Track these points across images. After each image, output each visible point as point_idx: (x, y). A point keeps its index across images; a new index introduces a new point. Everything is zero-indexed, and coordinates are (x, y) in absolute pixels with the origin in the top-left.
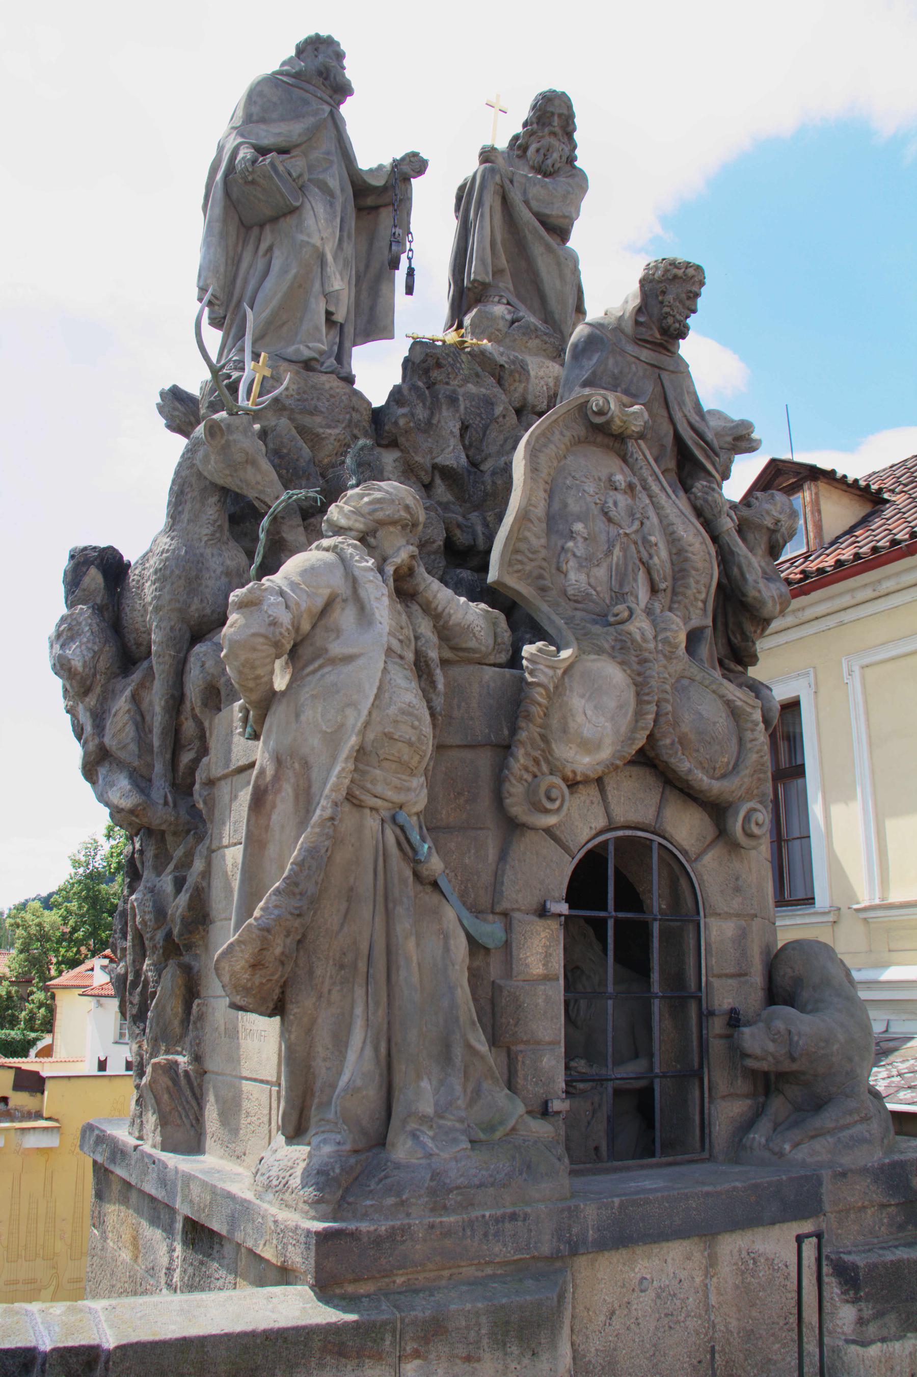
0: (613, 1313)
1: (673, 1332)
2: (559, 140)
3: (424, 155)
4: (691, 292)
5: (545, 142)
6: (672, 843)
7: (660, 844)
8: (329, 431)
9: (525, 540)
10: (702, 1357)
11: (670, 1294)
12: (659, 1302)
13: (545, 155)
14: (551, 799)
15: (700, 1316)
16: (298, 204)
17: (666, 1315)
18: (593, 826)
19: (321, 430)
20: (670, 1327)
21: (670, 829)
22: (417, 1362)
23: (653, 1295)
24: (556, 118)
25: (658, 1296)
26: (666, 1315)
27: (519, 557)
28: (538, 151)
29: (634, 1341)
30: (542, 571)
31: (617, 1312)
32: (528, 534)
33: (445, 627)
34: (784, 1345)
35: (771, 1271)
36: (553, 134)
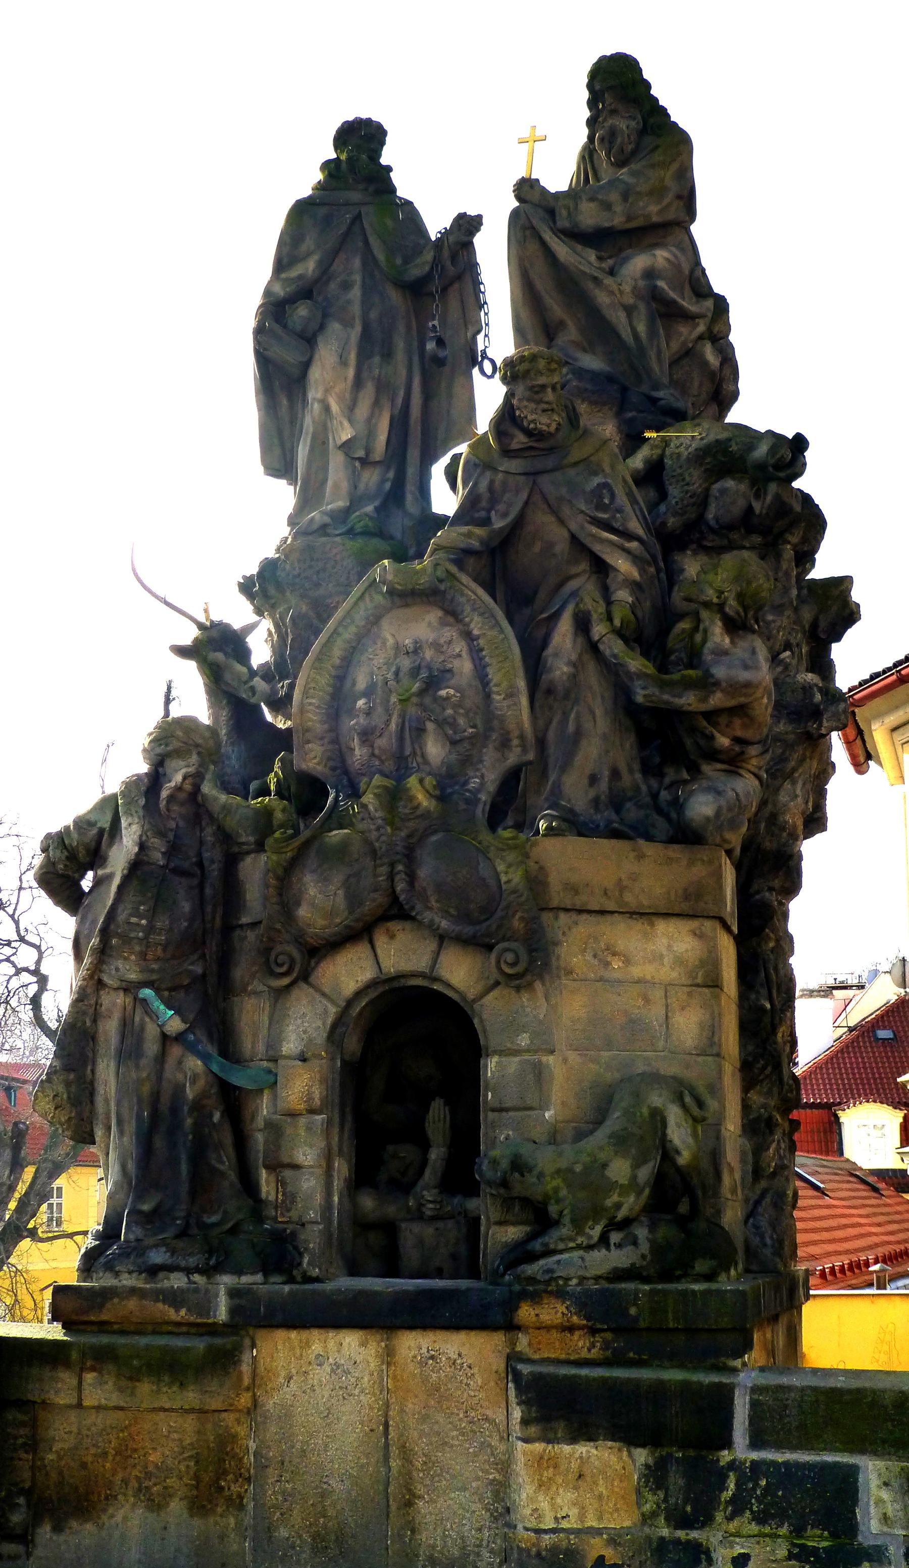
0: (291, 1378)
1: (345, 1402)
3: (472, 212)
4: (533, 387)
10: (374, 1427)
11: (344, 1371)
12: (333, 1376)
15: (374, 1394)
17: (341, 1388)
18: (359, 979)
20: (344, 1398)
22: (95, 1374)
23: (328, 1370)
25: (333, 1371)
26: (341, 1388)
29: (309, 1403)
35: (452, 1369)
36: (614, 112)
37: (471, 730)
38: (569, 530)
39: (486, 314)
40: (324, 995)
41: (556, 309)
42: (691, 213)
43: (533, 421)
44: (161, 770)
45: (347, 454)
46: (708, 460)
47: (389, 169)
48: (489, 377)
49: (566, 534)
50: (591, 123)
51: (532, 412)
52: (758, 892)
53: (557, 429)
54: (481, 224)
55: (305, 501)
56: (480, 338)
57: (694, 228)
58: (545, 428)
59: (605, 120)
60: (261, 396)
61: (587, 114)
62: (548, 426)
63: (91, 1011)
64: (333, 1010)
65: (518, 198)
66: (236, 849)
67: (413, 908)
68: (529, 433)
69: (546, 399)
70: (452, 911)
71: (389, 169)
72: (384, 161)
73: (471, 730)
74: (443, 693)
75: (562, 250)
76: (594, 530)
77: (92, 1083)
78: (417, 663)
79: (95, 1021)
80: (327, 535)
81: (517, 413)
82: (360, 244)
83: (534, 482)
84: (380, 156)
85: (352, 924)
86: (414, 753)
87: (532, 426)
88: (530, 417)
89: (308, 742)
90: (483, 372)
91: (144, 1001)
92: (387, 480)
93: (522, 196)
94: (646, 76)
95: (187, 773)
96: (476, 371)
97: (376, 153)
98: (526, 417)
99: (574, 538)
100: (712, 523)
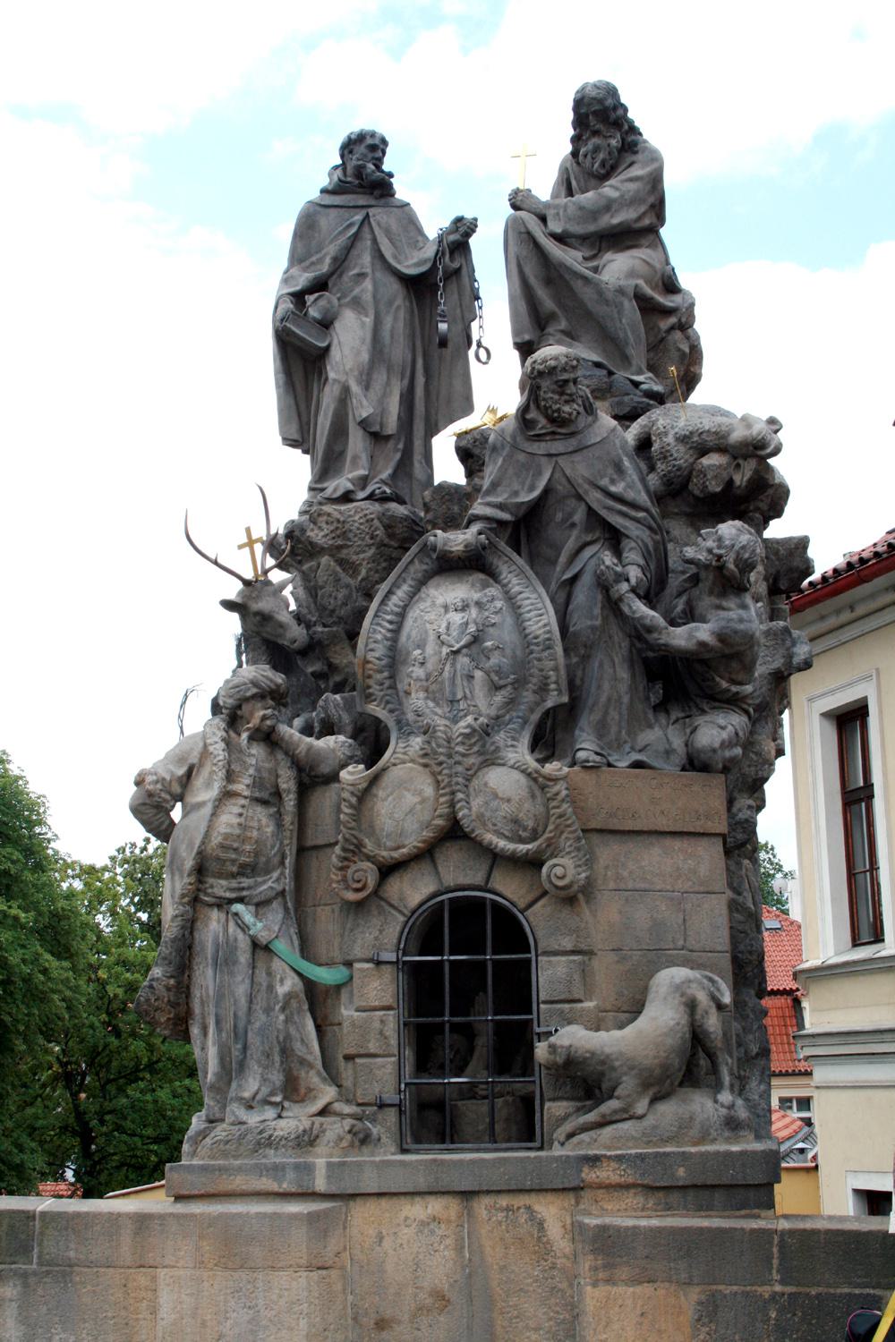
2: (605, 137)
3: (469, 215)
5: (590, 146)
6: (504, 898)
7: (491, 900)
8: (362, 556)
9: (370, 677)
13: (593, 158)
14: (359, 881)
16: (324, 345)
19: (355, 557)
21: (499, 887)
24: (591, 117)
27: (371, 691)
28: (585, 156)
30: (388, 698)
31: (386, 1238)
32: (371, 672)
33: (298, 761)
34: (536, 1281)
37: (512, 677)
38: (587, 503)
39: (480, 308)
40: (392, 906)
41: (548, 303)
42: (661, 218)
43: (558, 410)
44: (239, 712)
45: (364, 429)
46: (695, 439)
47: (391, 175)
48: (485, 363)
49: (583, 507)
50: (576, 140)
51: (556, 403)
52: (740, 810)
53: (576, 417)
54: (476, 226)
55: (324, 471)
56: (475, 325)
57: (663, 232)
58: (567, 416)
59: (588, 139)
60: (281, 376)
61: (571, 132)
62: (570, 414)
63: (189, 925)
64: (402, 919)
65: (515, 207)
66: (306, 780)
67: (473, 831)
68: (552, 420)
69: (569, 392)
70: (507, 833)
71: (391, 175)
72: (386, 167)
73: (512, 677)
74: (489, 644)
75: (555, 250)
76: (611, 503)
77: (188, 987)
78: (465, 620)
79: (191, 933)
80: (352, 501)
81: (543, 403)
82: (369, 243)
83: (557, 462)
84: (382, 163)
85: (420, 845)
86: (465, 697)
87: (556, 415)
88: (555, 407)
89: (369, 687)
90: (478, 359)
91: (236, 914)
92: (398, 450)
93: (518, 203)
94: (623, 100)
95: (264, 715)
96: (471, 353)
97: (378, 163)
98: (551, 407)
99: (591, 512)
100: (697, 492)
